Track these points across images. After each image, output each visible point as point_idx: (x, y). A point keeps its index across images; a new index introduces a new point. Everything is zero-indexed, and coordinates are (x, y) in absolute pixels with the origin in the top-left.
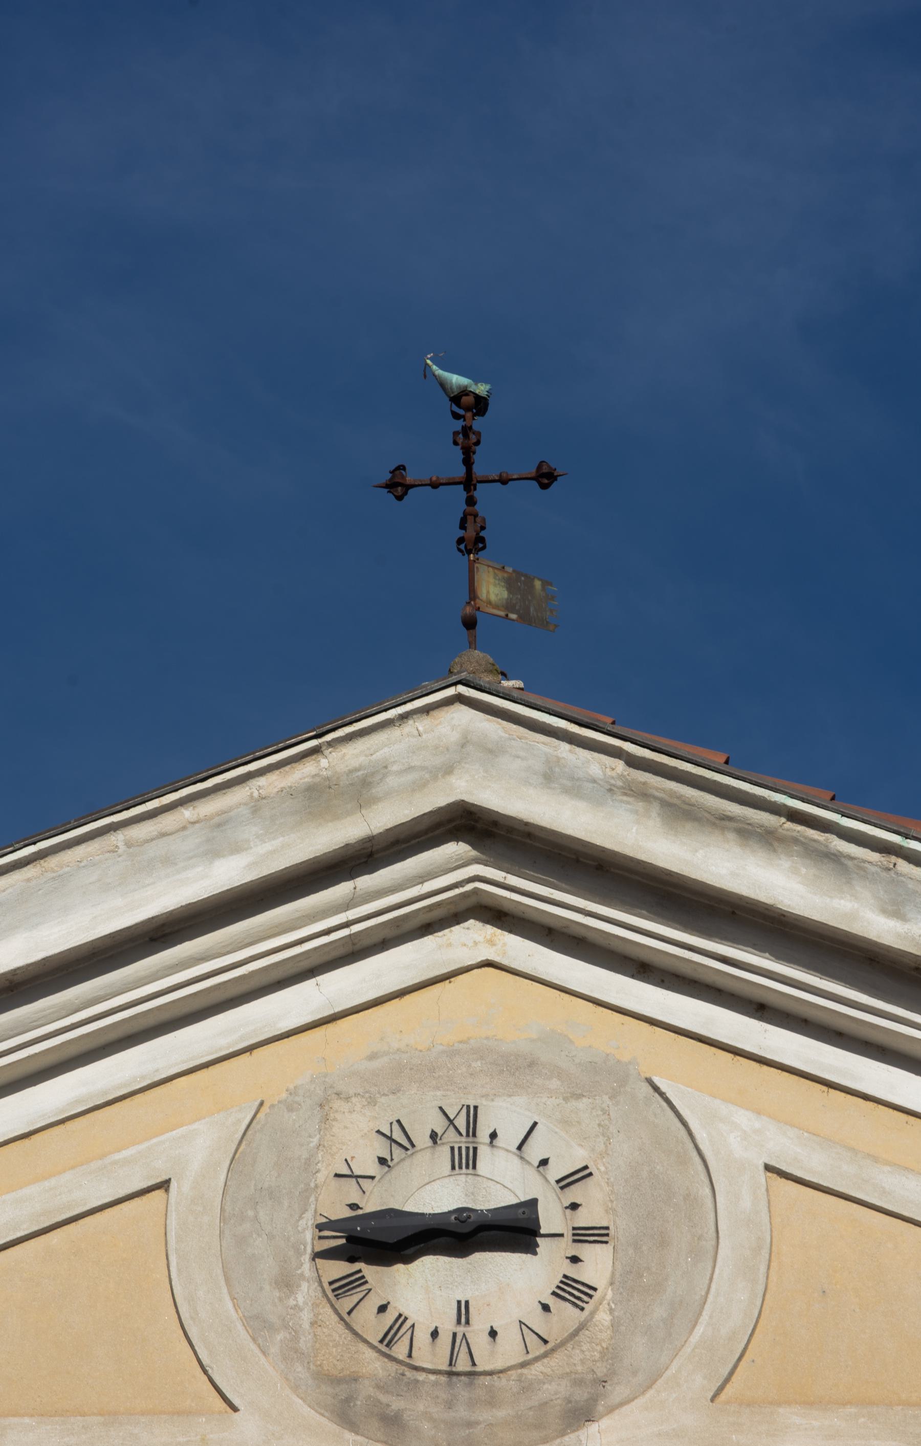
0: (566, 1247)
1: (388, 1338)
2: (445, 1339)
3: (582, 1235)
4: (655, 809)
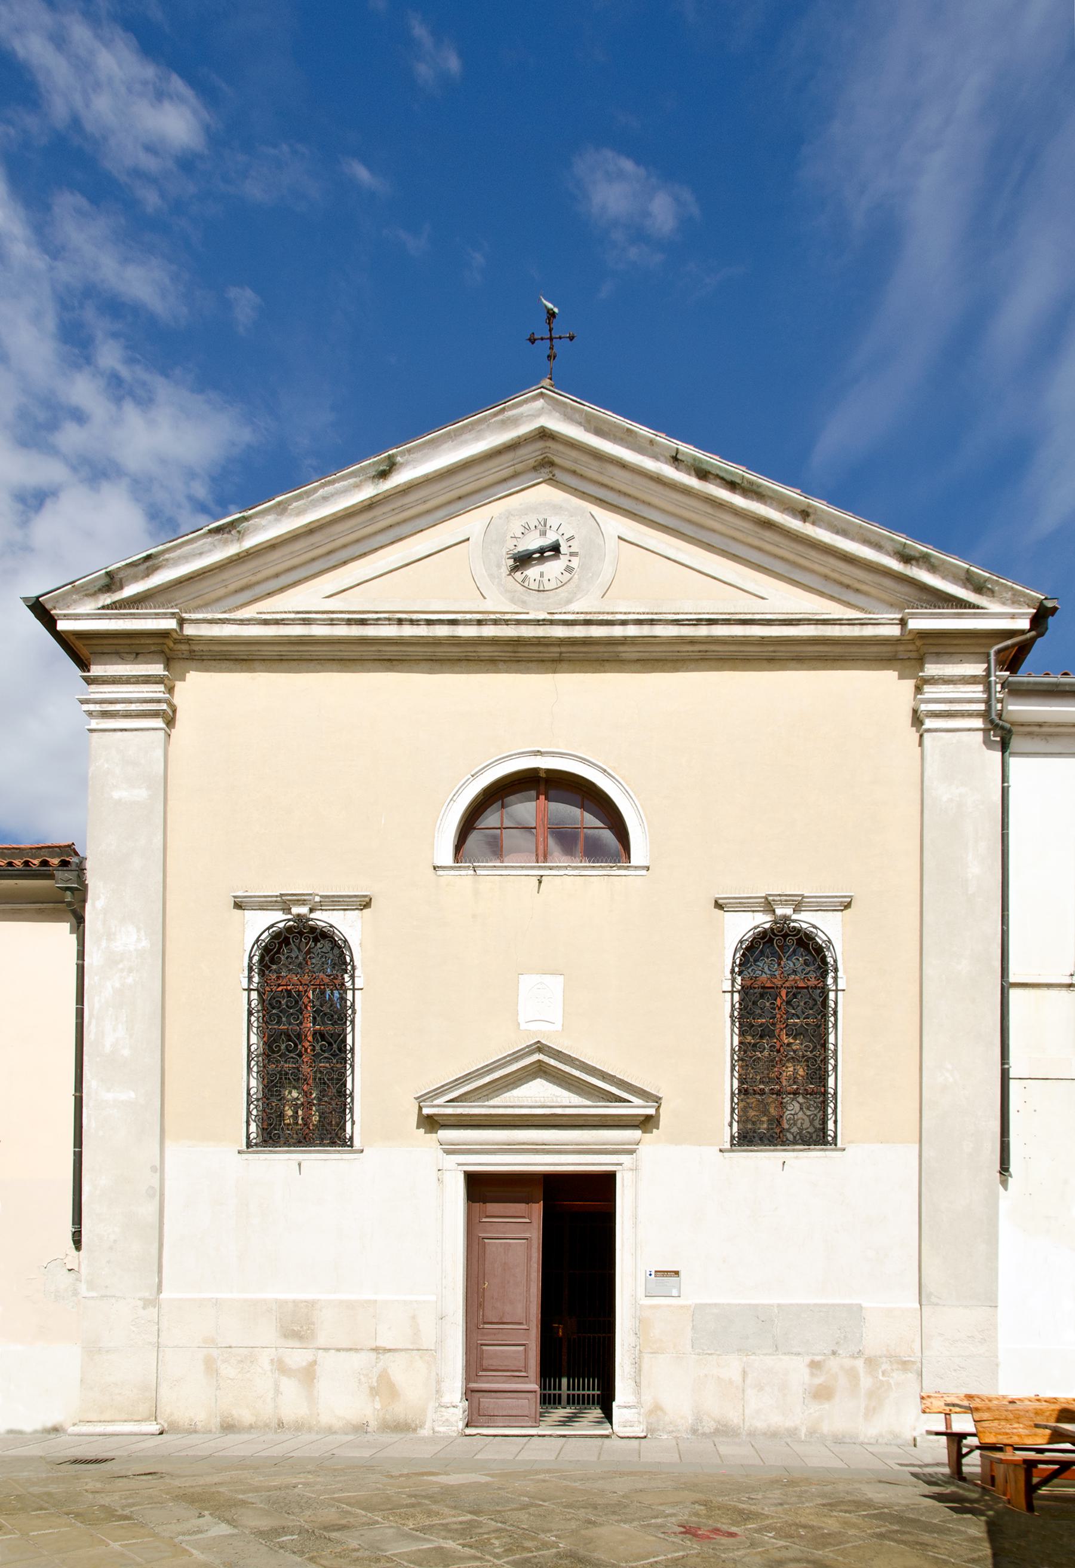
0: (568, 557)
1: (523, 581)
2: (537, 581)
3: (572, 554)
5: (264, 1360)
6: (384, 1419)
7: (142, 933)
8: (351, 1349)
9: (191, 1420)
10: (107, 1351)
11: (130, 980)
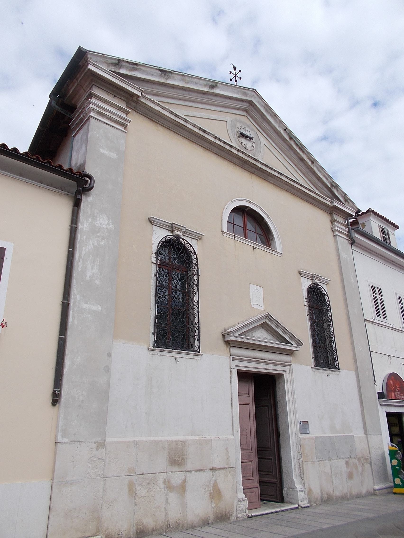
4: (265, 109)
5: (160, 482)
6: (217, 513)
7: (111, 221)
8: (201, 470)
9: (119, 531)
10: (71, 484)
11: (102, 243)
